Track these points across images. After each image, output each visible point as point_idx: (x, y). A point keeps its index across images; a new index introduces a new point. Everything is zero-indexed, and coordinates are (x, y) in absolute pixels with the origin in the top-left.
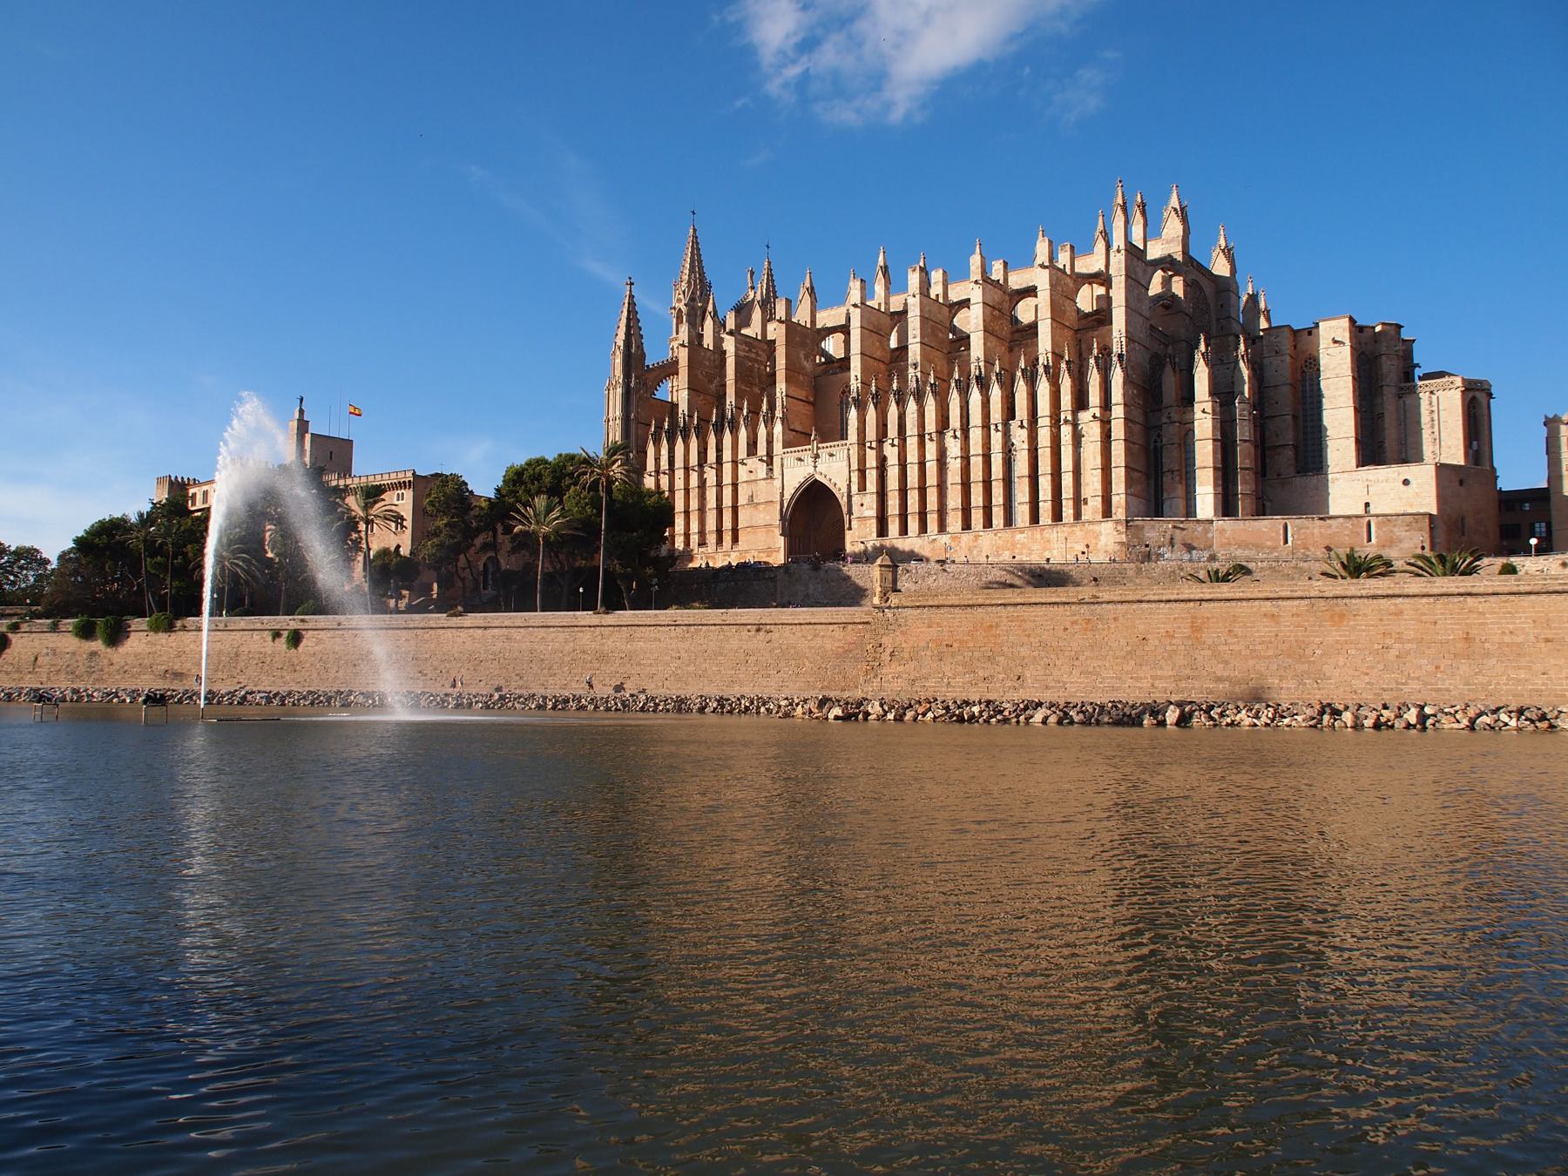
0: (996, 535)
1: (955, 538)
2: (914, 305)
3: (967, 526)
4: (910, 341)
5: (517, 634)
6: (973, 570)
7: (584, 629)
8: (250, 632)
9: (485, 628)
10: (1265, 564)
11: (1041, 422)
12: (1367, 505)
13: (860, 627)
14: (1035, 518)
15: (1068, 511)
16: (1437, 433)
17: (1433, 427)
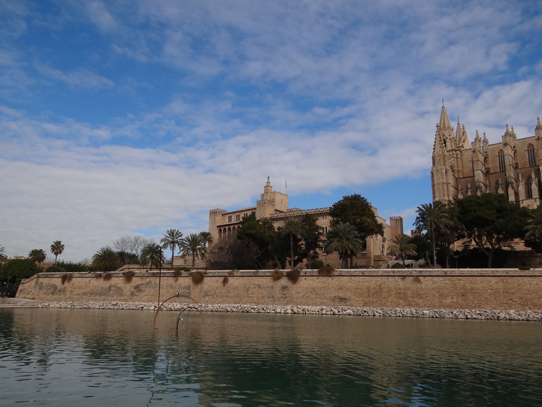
8: (386, 277)
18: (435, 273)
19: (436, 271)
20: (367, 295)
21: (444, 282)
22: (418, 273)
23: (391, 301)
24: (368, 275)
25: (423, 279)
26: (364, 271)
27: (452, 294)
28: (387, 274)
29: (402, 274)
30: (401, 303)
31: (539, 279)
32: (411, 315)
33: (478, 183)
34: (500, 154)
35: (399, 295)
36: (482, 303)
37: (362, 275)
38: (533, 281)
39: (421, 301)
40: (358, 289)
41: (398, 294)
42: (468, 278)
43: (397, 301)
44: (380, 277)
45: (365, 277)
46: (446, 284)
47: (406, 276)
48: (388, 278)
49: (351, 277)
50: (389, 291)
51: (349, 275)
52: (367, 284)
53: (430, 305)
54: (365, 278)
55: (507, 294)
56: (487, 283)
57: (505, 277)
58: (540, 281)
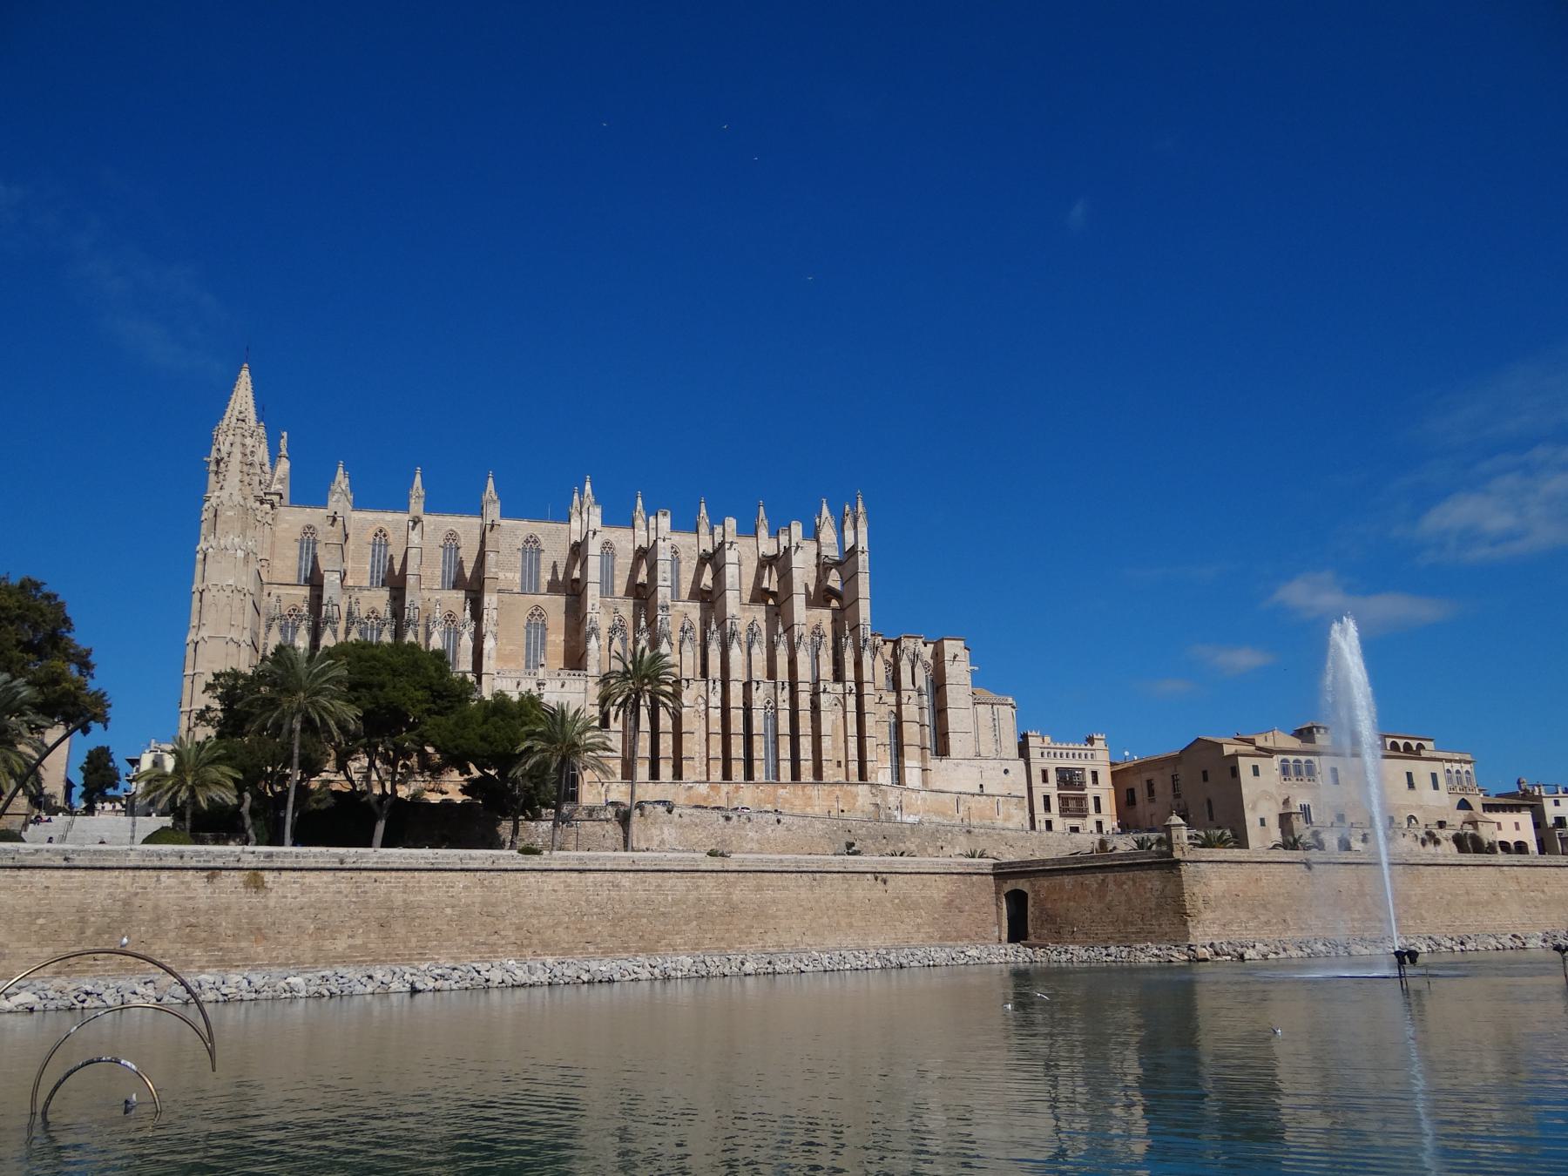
0: (758, 788)
1: (714, 786)
2: (664, 548)
3: (727, 775)
4: (660, 582)
5: (626, 880)
6: (802, 823)
7: (707, 874)
8: (151, 873)
9: (580, 871)
10: (982, 830)
11: (801, 687)
12: (981, 786)
13: (955, 877)
14: (796, 775)
15: (829, 771)
16: (997, 733)
17: (995, 730)
18: (312, 860)
19: (315, 856)
20: (72, 936)
21: (333, 888)
22: (262, 859)
23: (161, 951)
24: (87, 864)
25: (272, 879)
26: (73, 851)
27: (352, 923)
28: (158, 864)
29: (209, 861)
30: (197, 958)
31: (560, 877)
32: (254, 996)
33: (330, 608)
34: (378, 539)
35: (191, 931)
36: (430, 944)
37: (64, 864)
38: (546, 882)
39: (260, 949)
40: (39, 915)
41: (188, 930)
42: (400, 874)
43: (181, 953)
44: (130, 873)
45: (73, 873)
46: (340, 892)
47: (220, 869)
48: (158, 877)
49: (15, 873)
50: (158, 918)
51: (10, 863)
52: (77, 896)
53: (288, 959)
54: (71, 877)
55: (489, 919)
56: (444, 889)
57: (487, 874)
58: (560, 882)
